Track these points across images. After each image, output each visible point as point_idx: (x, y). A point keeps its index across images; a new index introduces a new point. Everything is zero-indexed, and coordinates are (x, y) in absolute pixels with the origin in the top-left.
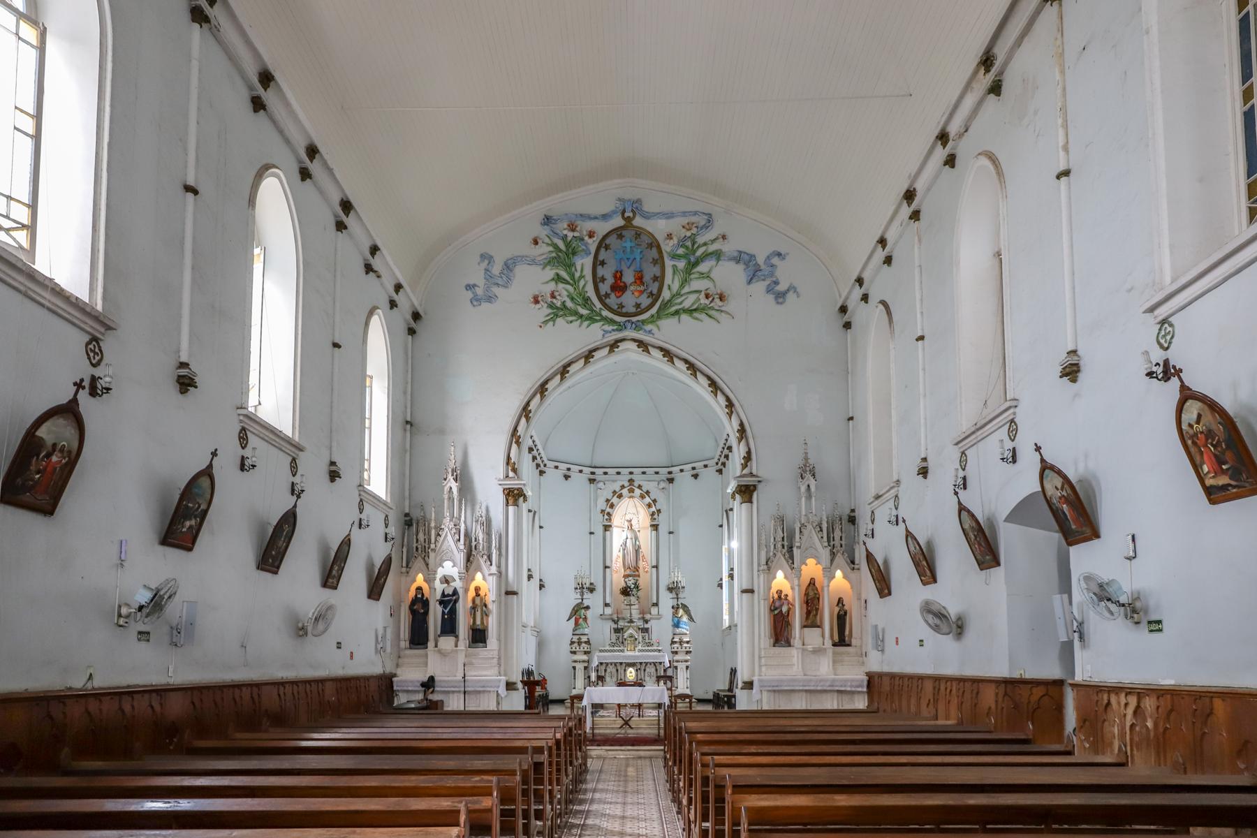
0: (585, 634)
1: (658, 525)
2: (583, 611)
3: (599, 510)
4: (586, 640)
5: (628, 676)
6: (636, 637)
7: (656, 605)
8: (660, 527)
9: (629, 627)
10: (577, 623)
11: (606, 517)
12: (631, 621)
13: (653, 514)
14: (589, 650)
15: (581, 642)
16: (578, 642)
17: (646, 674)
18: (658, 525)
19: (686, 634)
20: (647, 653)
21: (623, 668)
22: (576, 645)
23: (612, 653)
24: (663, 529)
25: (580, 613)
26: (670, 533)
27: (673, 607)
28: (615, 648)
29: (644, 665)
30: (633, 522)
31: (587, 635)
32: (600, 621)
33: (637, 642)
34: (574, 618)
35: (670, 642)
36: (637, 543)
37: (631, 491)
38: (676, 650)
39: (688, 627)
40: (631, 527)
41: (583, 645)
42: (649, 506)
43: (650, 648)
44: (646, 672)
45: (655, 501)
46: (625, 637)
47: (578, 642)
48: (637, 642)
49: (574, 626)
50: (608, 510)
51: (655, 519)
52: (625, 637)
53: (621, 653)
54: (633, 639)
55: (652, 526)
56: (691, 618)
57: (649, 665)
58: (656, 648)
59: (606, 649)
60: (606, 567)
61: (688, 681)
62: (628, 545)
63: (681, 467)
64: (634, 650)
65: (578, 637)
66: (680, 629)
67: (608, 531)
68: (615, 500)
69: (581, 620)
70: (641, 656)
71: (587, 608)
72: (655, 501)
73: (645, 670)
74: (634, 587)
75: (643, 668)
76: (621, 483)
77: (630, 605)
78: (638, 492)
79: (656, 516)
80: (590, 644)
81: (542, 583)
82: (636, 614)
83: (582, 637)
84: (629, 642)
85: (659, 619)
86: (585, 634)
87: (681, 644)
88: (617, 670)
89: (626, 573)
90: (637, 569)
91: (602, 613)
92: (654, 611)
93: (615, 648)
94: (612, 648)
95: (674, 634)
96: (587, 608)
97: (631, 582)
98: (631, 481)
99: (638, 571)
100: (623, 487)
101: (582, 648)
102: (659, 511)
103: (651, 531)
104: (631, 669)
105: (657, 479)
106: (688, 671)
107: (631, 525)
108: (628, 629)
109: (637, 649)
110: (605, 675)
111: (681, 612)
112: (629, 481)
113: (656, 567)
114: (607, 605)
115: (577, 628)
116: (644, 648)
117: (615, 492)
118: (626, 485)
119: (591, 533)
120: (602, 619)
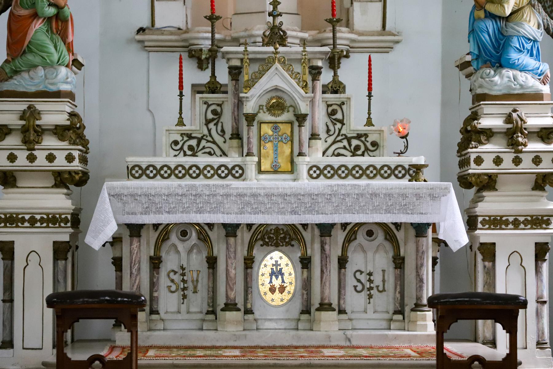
0: (57, 94)
4: (62, 119)
5: (264, 289)
6: (304, 108)
14: (76, 165)
15: (40, 132)
16: (25, 130)
17: (350, 282)
19: (538, 96)
20: (350, 181)
21: (242, 252)
22: (13, 141)
23: (187, 182)
28: (202, 160)
29: (340, 236)
31: (70, 95)
33: (306, 132)
35: (459, 137)
38: (487, 167)
39: (545, 67)
41: (50, 142)
43: (364, 161)
44: (351, 268)
46: (249, 108)
47: (25, 130)
48: (306, 132)
52: (249, 108)
53: (230, 182)
54: (286, 116)
57: (361, 237)
58: (393, 161)
59: (158, 161)
61: (545, 309)
64: (293, 170)
65: (21, 106)
66: (508, 73)
69: (38, 26)
70: (329, 197)
73: (342, 262)
75: (335, 252)
80: (85, 143)
83: (41, 105)
84: (267, 130)
86: (57, 94)
87: (513, 144)
88: (212, 262)
93: (202, 160)
94: (188, 161)
95: (479, 98)
101: (41, 156)
104: (276, 255)
106: (545, 267)
108: (261, 74)
109: (303, 164)
110: (153, 285)
115: (19, 62)
116: (336, 162)
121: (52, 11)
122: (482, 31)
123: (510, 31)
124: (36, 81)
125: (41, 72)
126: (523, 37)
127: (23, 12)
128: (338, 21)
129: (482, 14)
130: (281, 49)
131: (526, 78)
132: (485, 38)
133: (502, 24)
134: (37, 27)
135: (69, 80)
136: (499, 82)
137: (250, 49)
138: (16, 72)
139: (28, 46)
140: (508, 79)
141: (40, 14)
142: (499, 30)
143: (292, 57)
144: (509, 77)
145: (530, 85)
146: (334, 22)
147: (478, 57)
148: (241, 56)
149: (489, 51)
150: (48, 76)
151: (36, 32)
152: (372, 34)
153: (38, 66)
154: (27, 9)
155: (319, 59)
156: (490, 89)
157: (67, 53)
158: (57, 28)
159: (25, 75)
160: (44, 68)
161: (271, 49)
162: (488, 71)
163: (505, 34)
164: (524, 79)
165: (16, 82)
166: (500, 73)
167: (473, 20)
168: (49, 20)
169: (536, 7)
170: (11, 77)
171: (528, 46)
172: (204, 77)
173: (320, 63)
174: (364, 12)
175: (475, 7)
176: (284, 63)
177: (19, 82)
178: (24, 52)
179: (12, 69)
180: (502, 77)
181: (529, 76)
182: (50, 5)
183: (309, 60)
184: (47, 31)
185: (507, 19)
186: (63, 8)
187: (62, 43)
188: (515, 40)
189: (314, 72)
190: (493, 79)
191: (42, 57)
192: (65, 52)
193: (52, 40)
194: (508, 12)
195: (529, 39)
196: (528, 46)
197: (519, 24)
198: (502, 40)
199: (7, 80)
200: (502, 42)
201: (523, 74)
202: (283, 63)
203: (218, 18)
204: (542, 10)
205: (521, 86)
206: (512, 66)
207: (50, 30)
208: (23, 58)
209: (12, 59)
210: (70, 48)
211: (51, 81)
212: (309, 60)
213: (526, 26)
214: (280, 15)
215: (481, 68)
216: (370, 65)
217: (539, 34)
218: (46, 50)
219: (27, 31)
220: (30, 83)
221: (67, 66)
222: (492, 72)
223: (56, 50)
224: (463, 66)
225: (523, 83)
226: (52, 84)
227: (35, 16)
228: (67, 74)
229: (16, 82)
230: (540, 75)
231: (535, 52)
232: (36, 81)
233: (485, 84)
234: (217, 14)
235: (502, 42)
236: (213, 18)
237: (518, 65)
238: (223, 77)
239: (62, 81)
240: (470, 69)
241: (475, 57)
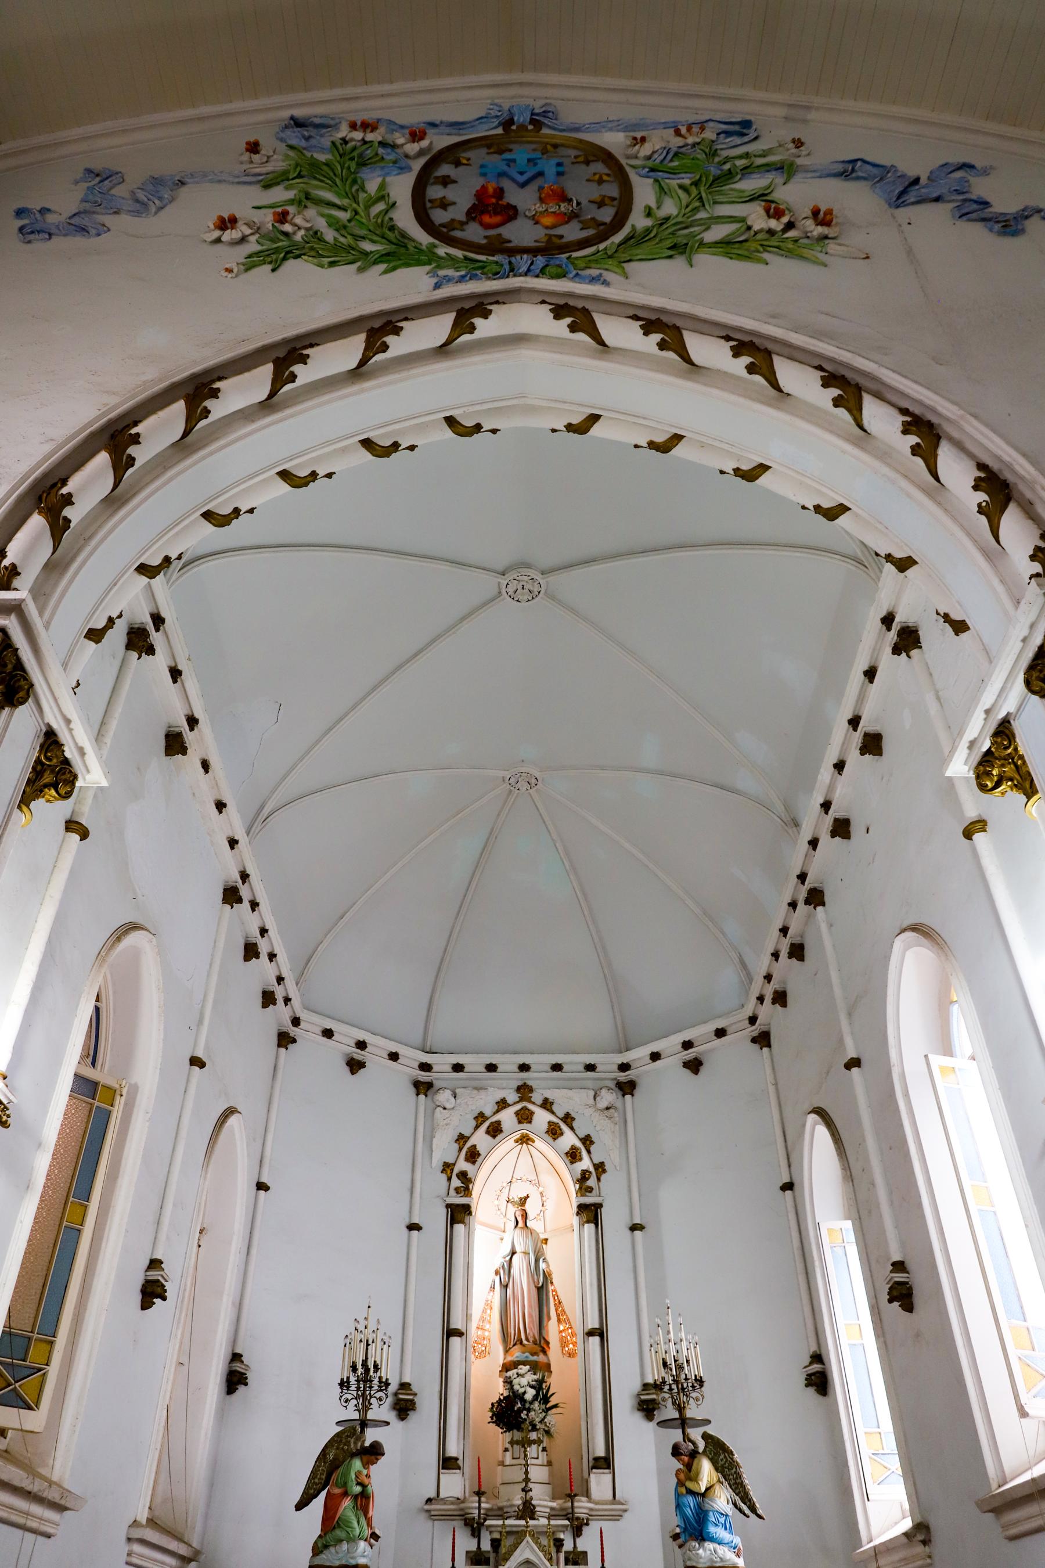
1: (599, 1206)
2: (357, 1464)
3: (437, 1161)
7: (605, 1463)
8: (605, 1213)
9: (518, 1536)
10: (330, 1521)
11: (456, 1182)
12: (528, 1510)
13: (583, 1177)
18: (600, 1206)
24: (614, 1218)
25: (347, 1474)
26: (634, 1228)
27: (676, 1451)
30: (531, 1207)
32: (424, 1525)
34: (323, 1495)
36: (542, 1266)
37: (525, 1117)
40: (522, 1220)
42: (573, 1156)
45: (587, 1141)
49: (317, 1531)
50: (462, 1165)
51: (590, 1190)
55: (582, 1208)
56: (746, 1498)
60: (451, 1333)
62: (515, 1270)
63: (654, 1047)
66: (710, 1546)
67: (462, 1222)
68: (480, 1139)
69: (347, 1503)
71: (375, 1452)
72: (587, 1141)
74: (535, 1398)
76: (499, 1095)
77: (525, 1443)
78: (542, 1118)
79: (592, 1182)
81: (238, 1367)
82: (542, 1499)
85: (616, 1517)
89: (509, 1358)
90: (541, 1345)
91: (432, 1494)
92: (599, 1483)
96: (375, 1452)
97: (524, 1381)
98: (524, 1091)
99: (544, 1352)
100: (503, 1104)
102: (600, 1168)
103: (581, 1225)
105: (590, 1084)
107: (525, 1216)
111: (706, 1471)
112: (519, 1089)
113: (600, 1333)
114: (448, 1463)
115: (329, 1537)
117: (480, 1118)
118: (510, 1101)
119: (413, 1227)
120: (432, 1516)
121: (358, 1489)
122: (685, 1506)
123: (707, 1507)
124: (340, 1555)
125: (345, 1546)
126: (717, 1511)
127: (337, 1491)
128: (576, 1495)
129: (683, 1490)
130: (531, 1522)
131: (724, 1551)
132: (688, 1512)
133: (700, 1499)
134: (346, 1504)
135: (366, 1553)
136: (703, 1555)
137: (507, 1522)
138: (326, 1547)
139: (337, 1522)
140: (709, 1552)
141: (349, 1492)
142: (698, 1505)
143: (540, 1530)
144: (710, 1550)
145: (728, 1558)
146: (571, 1497)
147: (685, 1530)
148: (499, 1529)
149: (693, 1525)
150: (350, 1551)
151: (345, 1509)
152: (605, 1503)
153: (342, 1541)
154: (340, 1488)
155: (561, 1531)
156: (697, 1562)
157: (366, 1528)
158: (361, 1504)
159: (332, 1549)
160: (348, 1542)
161: (523, 1522)
162: (694, 1544)
163: (703, 1508)
164: (722, 1552)
165: (324, 1556)
166: (703, 1546)
167: (678, 1496)
168: (356, 1497)
169: (724, 1483)
170: (321, 1552)
171: (722, 1520)
172: (472, 1545)
173: (562, 1536)
174: (598, 1483)
175: (678, 1484)
176: (533, 1535)
177: (327, 1556)
178: (334, 1528)
179: (323, 1544)
180: (705, 1550)
181: (726, 1549)
182: (358, 1484)
183: (554, 1533)
184: (353, 1507)
185: (703, 1495)
186: (367, 1486)
187: (364, 1519)
188: (711, 1514)
189: (557, 1544)
190: (698, 1552)
191: (347, 1532)
192: (365, 1527)
193: (356, 1515)
194: (703, 1490)
195: (722, 1514)
196: (722, 1520)
197: (712, 1500)
198: (701, 1514)
199: (317, 1555)
200: (702, 1516)
201: (721, 1547)
202: (532, 1536)
203: (483, 1493)
204: (728, 1487)
205: (721, 1558)
206: (712, 1540)
207: (355, 1506)
208: (333, 1533)
209: (325, 1534)
210: (369, 1524)
211: (352, 1555)
212: (554, 1533)
213: (718, 1502)
214: (531, 1490)
215: (688, 1541)
216: (602, 1537)
217: (729, 1509)
218: (350, 1525)
219: (337, 1510)
220: (335, 1558)
221: (366, 1540)
222: (697, 1545)
223: (359, 1524)
224: (675, 1537)
225: (722, 1556)
226: (352, 1558)
227: (345, 1494)
228: (365, 1549)
229: (324, 1556)
230: (734, 1549)
231: (728, 1526)
232: (340, 1555)
233: (693, 1557)
234: (482, 1490)
235: (702, 1516)
236: (479, 1493)
237: (717, 1539)
238: (486, 1546)
239: (360, 1554)
240: (680, 1541)
241: (682, 1530)
